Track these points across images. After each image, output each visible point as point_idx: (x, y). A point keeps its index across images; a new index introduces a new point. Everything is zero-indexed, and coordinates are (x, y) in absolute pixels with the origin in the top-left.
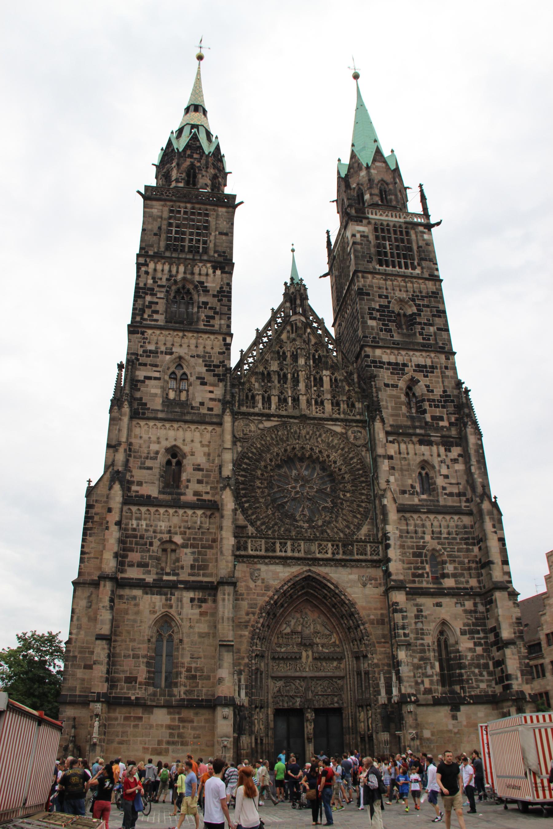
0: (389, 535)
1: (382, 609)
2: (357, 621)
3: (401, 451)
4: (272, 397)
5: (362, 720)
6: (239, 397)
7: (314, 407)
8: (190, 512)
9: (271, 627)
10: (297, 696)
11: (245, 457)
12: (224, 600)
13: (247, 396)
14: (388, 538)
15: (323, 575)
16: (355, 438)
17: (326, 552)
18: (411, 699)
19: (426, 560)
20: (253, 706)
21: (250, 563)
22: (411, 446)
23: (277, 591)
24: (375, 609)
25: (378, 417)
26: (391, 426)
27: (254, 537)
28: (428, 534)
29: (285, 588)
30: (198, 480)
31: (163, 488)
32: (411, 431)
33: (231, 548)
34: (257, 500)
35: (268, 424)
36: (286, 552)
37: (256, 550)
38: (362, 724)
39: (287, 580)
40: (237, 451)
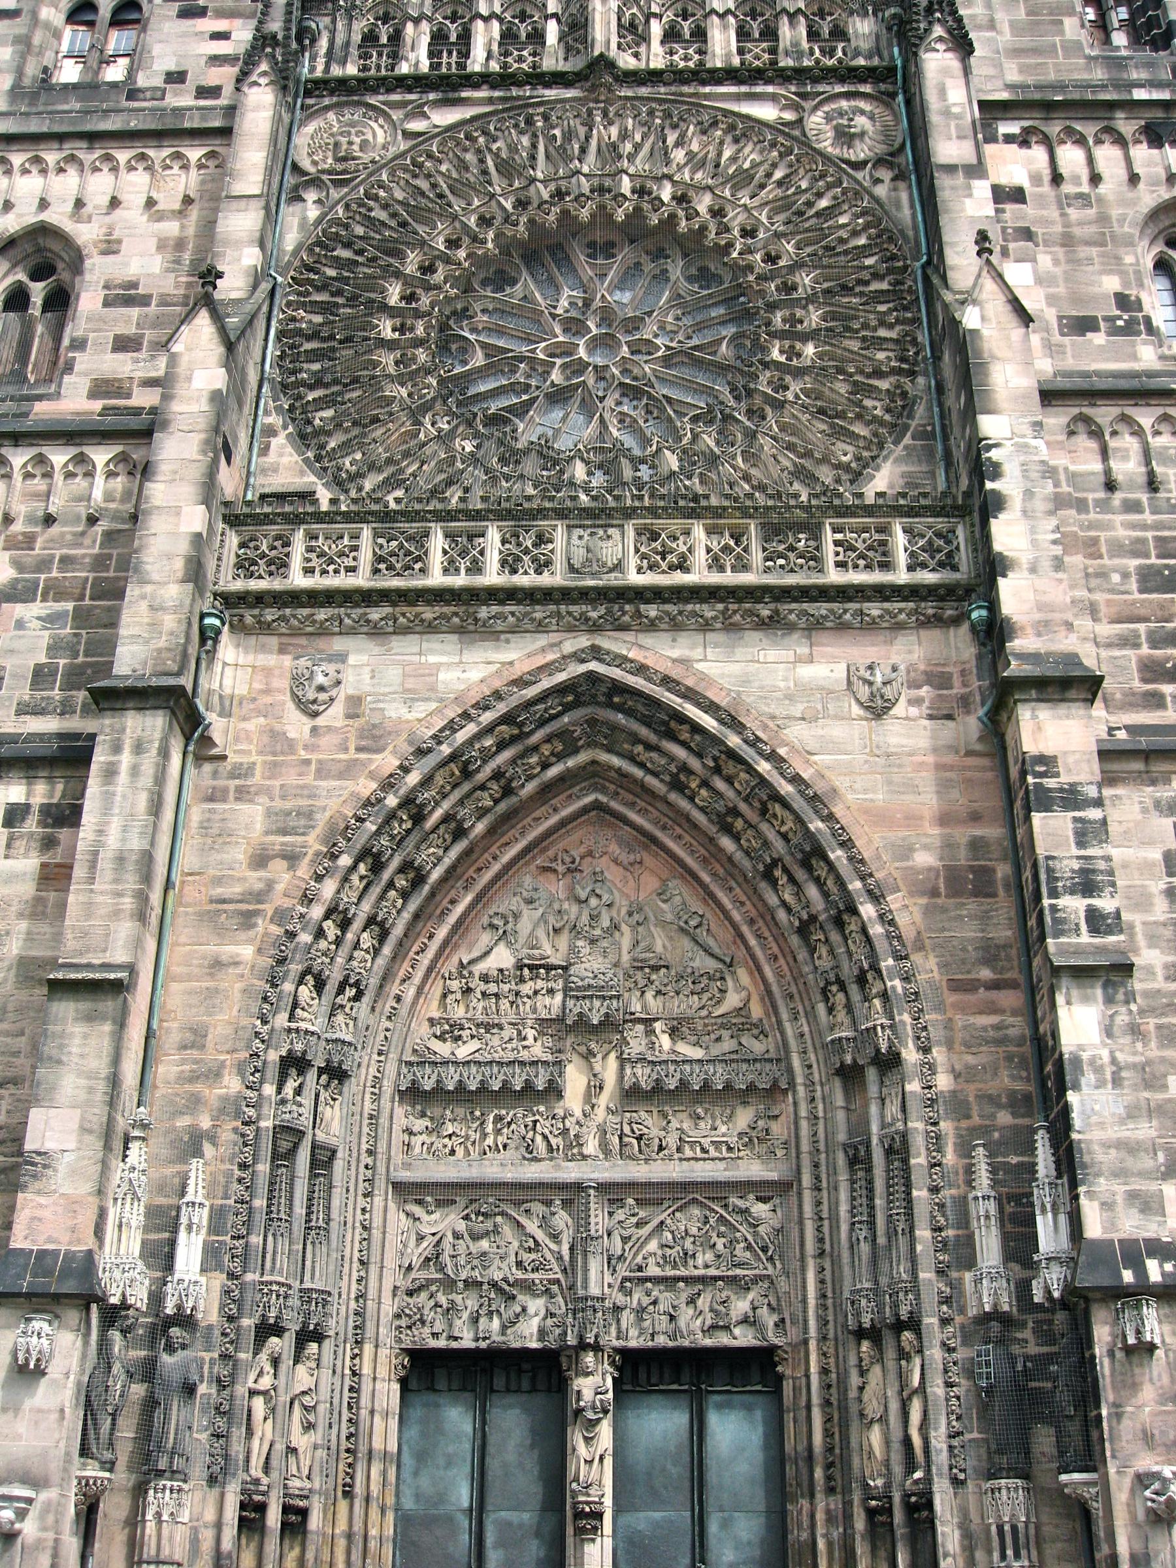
0: (994, 454)
1: (975, 817)
2: (841, 884)
3: (1064, 170)
5: (873, 1408)
6: (332, 42)
7: (656, 47)
10: (528, 1287)
12: (110, 772)
14: (996, 471)
16: (845, 136)
18: (1141, 1271)
20: (247, 1322)
21: (295, 633)
22: (1108, 156)
23: (421, 752)
25: (938, 31)
29: (461, 737)
30: (117, 338)
33: (183, 547)
39: (474, 696)
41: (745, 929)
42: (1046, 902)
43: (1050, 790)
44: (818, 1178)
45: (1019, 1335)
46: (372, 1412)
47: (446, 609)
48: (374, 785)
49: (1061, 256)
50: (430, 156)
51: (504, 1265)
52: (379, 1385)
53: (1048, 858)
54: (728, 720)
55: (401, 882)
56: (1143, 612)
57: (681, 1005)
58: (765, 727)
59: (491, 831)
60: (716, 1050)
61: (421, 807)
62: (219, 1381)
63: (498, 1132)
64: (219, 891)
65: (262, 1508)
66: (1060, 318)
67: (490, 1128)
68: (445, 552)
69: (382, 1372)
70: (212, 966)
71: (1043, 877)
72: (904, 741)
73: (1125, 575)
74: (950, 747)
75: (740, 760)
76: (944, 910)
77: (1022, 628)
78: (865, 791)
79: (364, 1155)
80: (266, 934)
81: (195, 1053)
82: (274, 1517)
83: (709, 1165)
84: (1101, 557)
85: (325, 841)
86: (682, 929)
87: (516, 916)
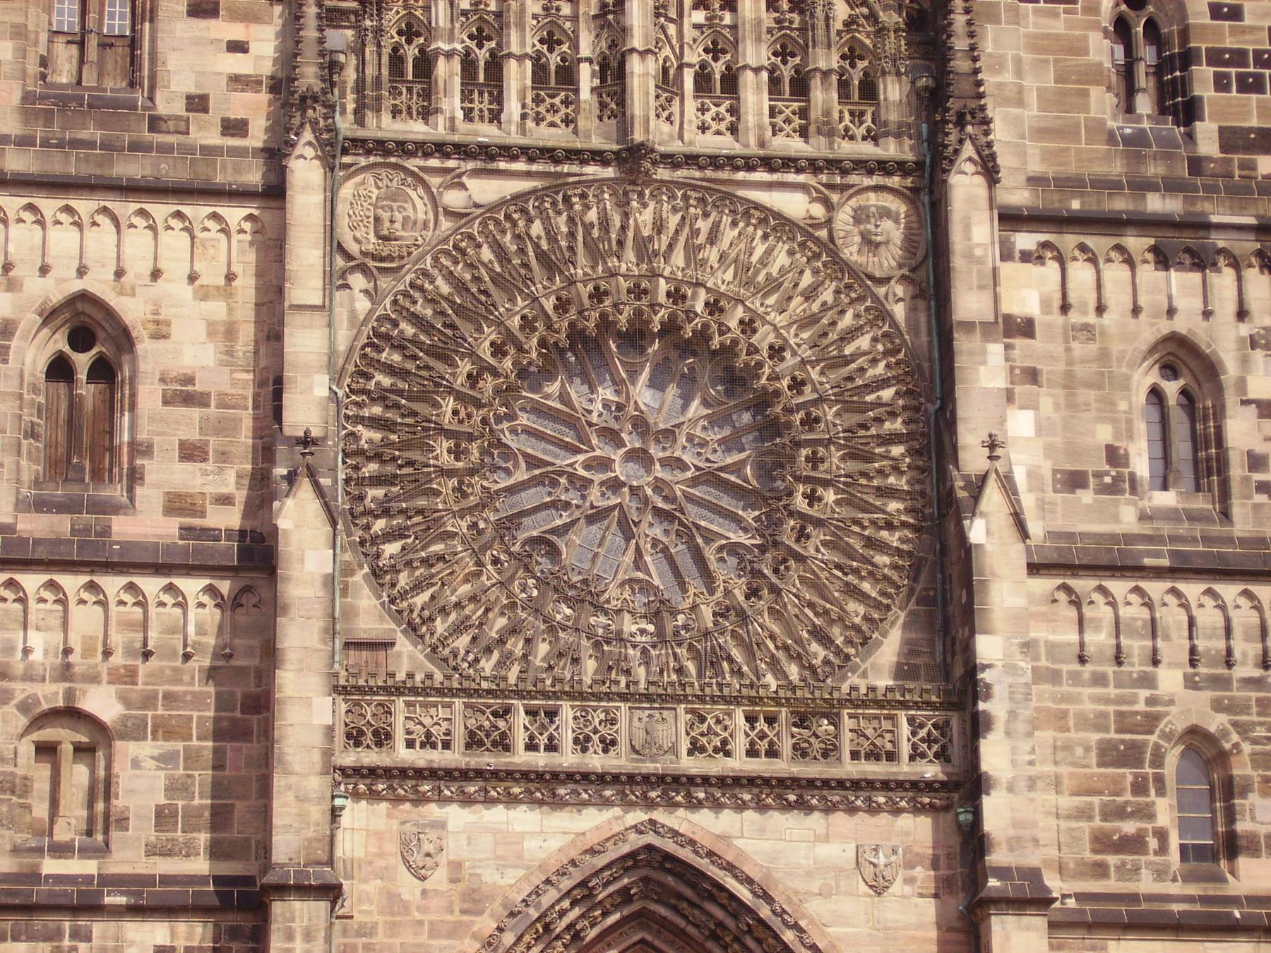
3: (1073, 298)
4: (512, 67)
7: (691, 105)
8: (151, 585)
11: (386, 337)
13: (397, 61)
15: (708, 843)
16: (870, 243)
17: (724, 749)
19: (1159, 780)
22: (1115, 274)
23: (512, 914)
26: (1034, 181)
27: (414, 691)
28: (1171, 665)
30: (182, 444)
31: (37, 483)
32: (1121, 204)
33: (318, 739)
34: (432, 527)
35: (487, 190)
36: (552, 747)
37: (429, 742)
40: (353, 313)
49: (1062, 400)
50: (471, 237)
54: (760, 893)
56: (1098, 786)
58: (789, 900)
66: (1055, 472)
73: (1087, 749)
75: (769, 928)
77: (999, 844)
84: (1068, 730)
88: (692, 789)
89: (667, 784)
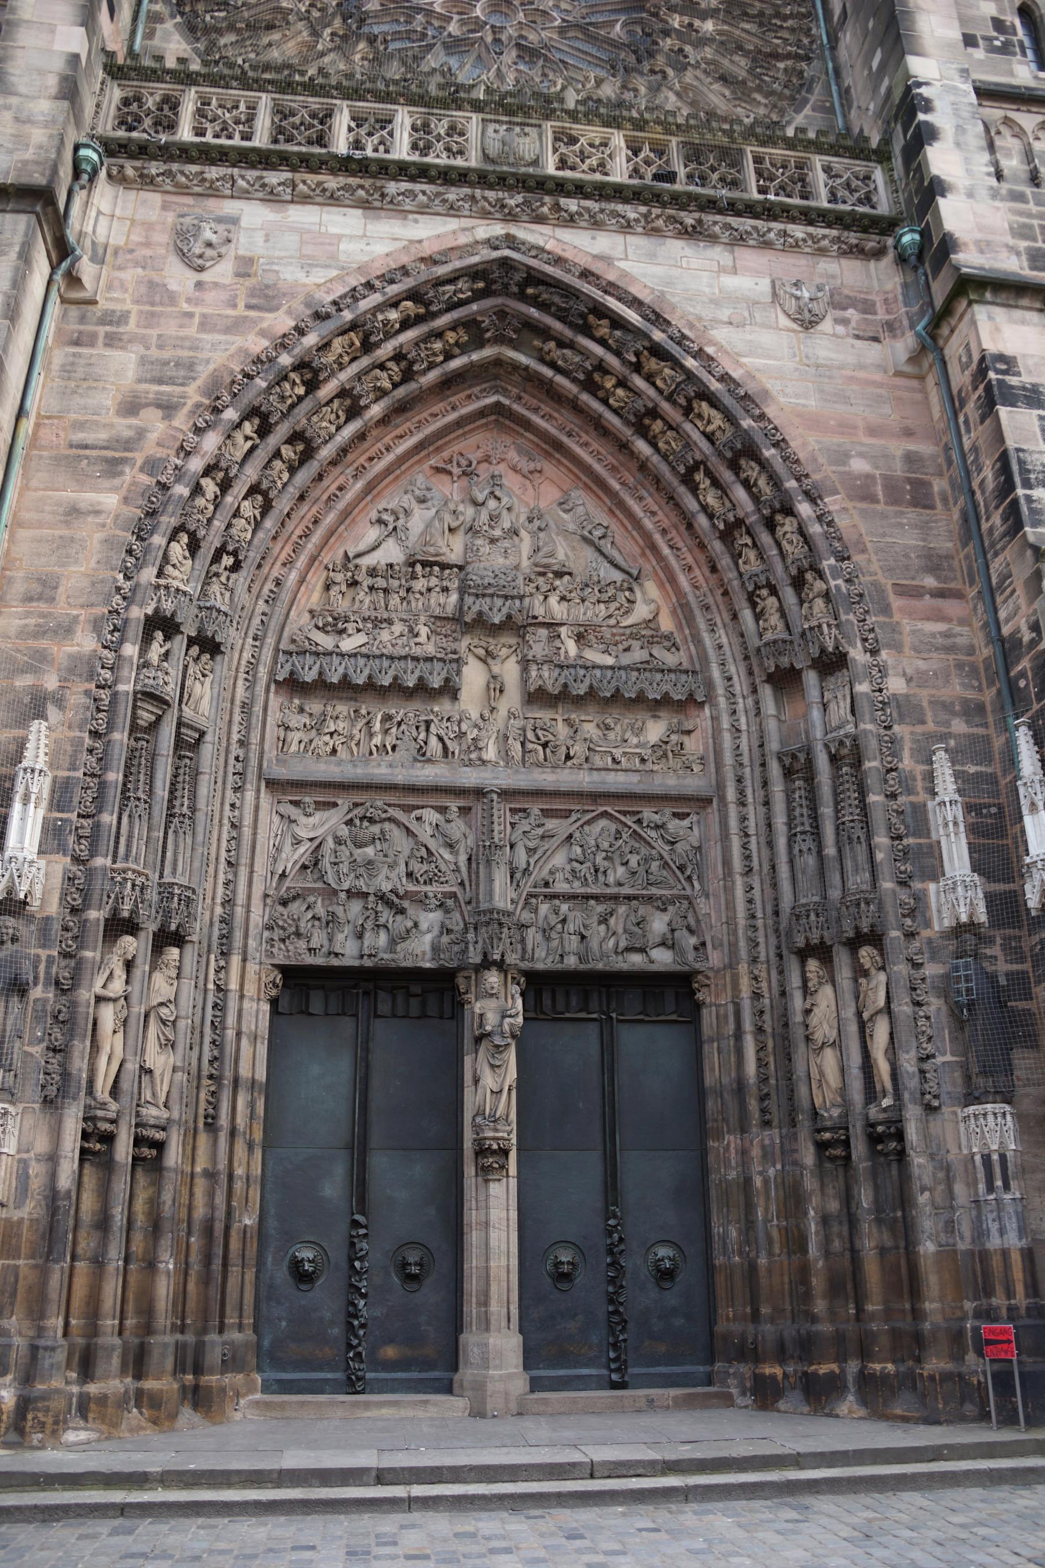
1: (908, 433)
2: (775, 481)
9: (283, 504)
10: (421, 901)
14: (928, 106)
15: (584, 262)
20: (96, 915)
21: (183, 190)
23: (319, 316)
24: (873, 431)
29: (364, 305)
38: (829, 1059)
41: (658, 537)
42: (1020, 492)
43: (1012, 387)
44: (742, 792)
45: (988, 952)
46: (239, 1034)
47: (351, 181)
48: (265, 343)
51: (393, 875)
52: (246, 1004)
53: (1018, 450)
55: (287, 452)
57: (585, 613)
58: (691, 326)
59: (384, 421)
60: (626, 660)
61: (316, 372)
62: (57, 983)
63: (386, 732)
64: (80, 436)
65: (109, 1139)
67: (377, 726)
68: (350, 130)
69: (251, 989)
70: (68, 514)
71: (1015, 467)
72: (833, 356)
74: (879, 366)
76: (884, 516)
78: (797, 396)
79: (234, 746)
80: (134, 483)
81: (43, 606)
82: (123, 1150)
83: (621, 777)
85: (207, 394)
86: (585, 539)
87: (407, 513)
88: (563, 201)
89: (529, 190)
